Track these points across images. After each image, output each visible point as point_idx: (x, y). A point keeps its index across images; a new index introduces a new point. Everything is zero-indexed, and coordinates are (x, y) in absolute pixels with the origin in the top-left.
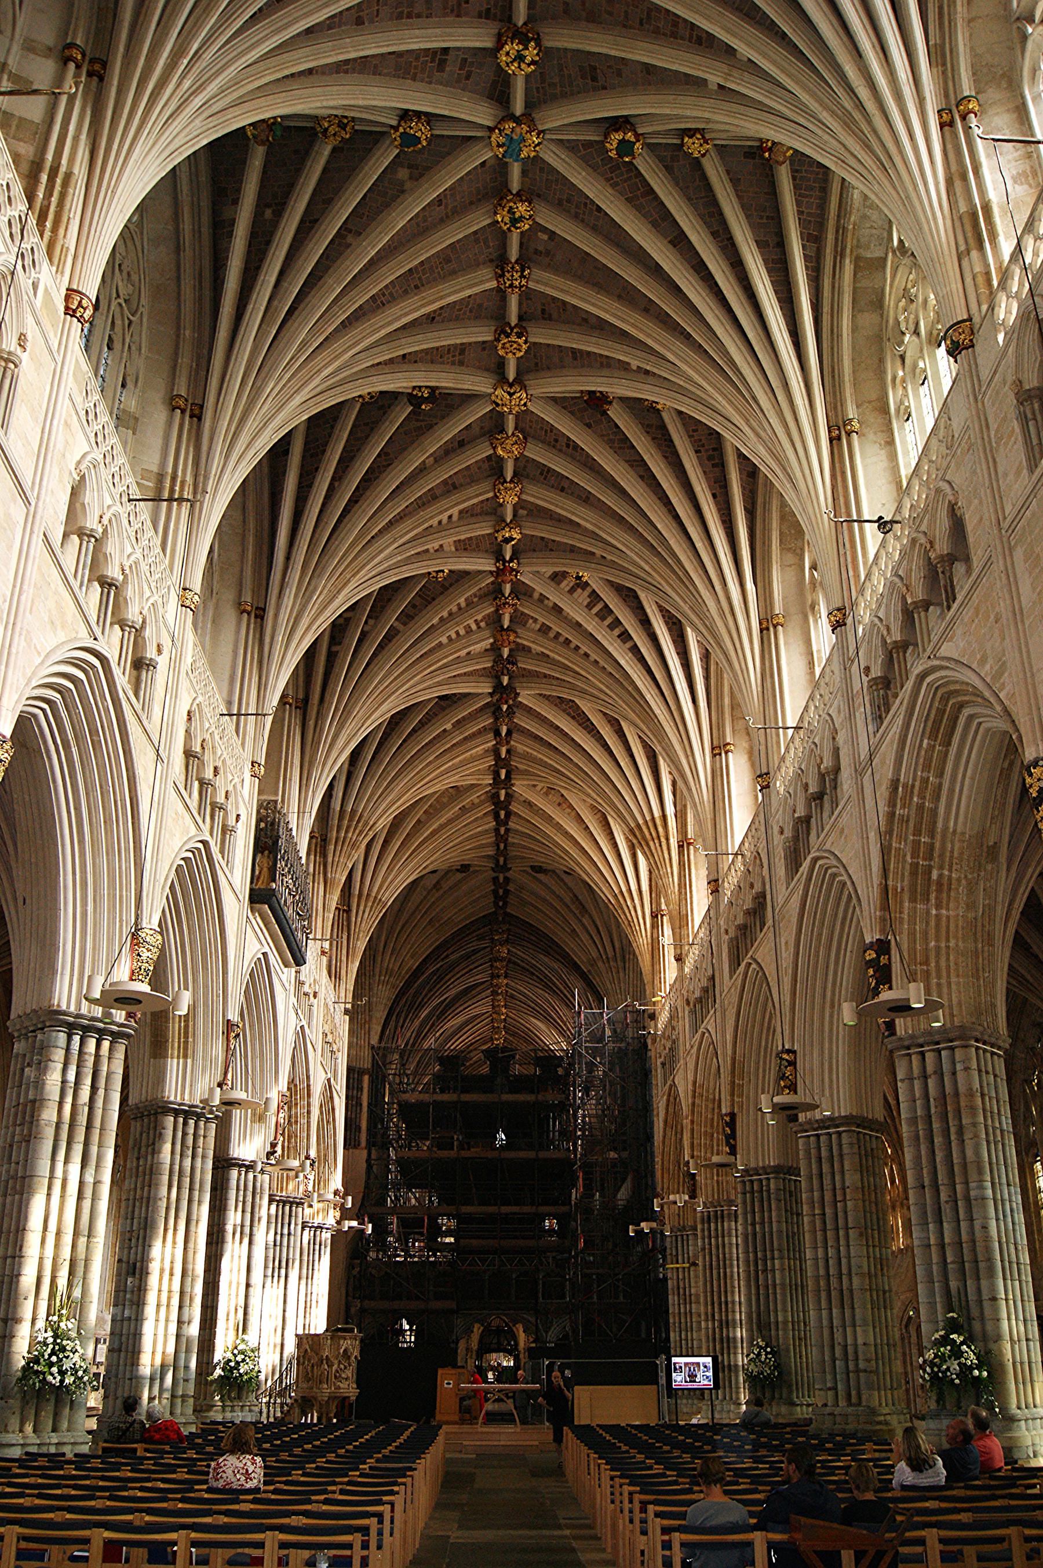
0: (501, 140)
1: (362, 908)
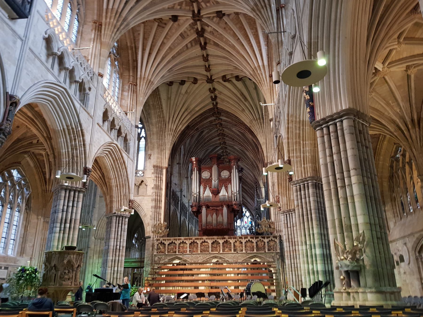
1: (142, 83)
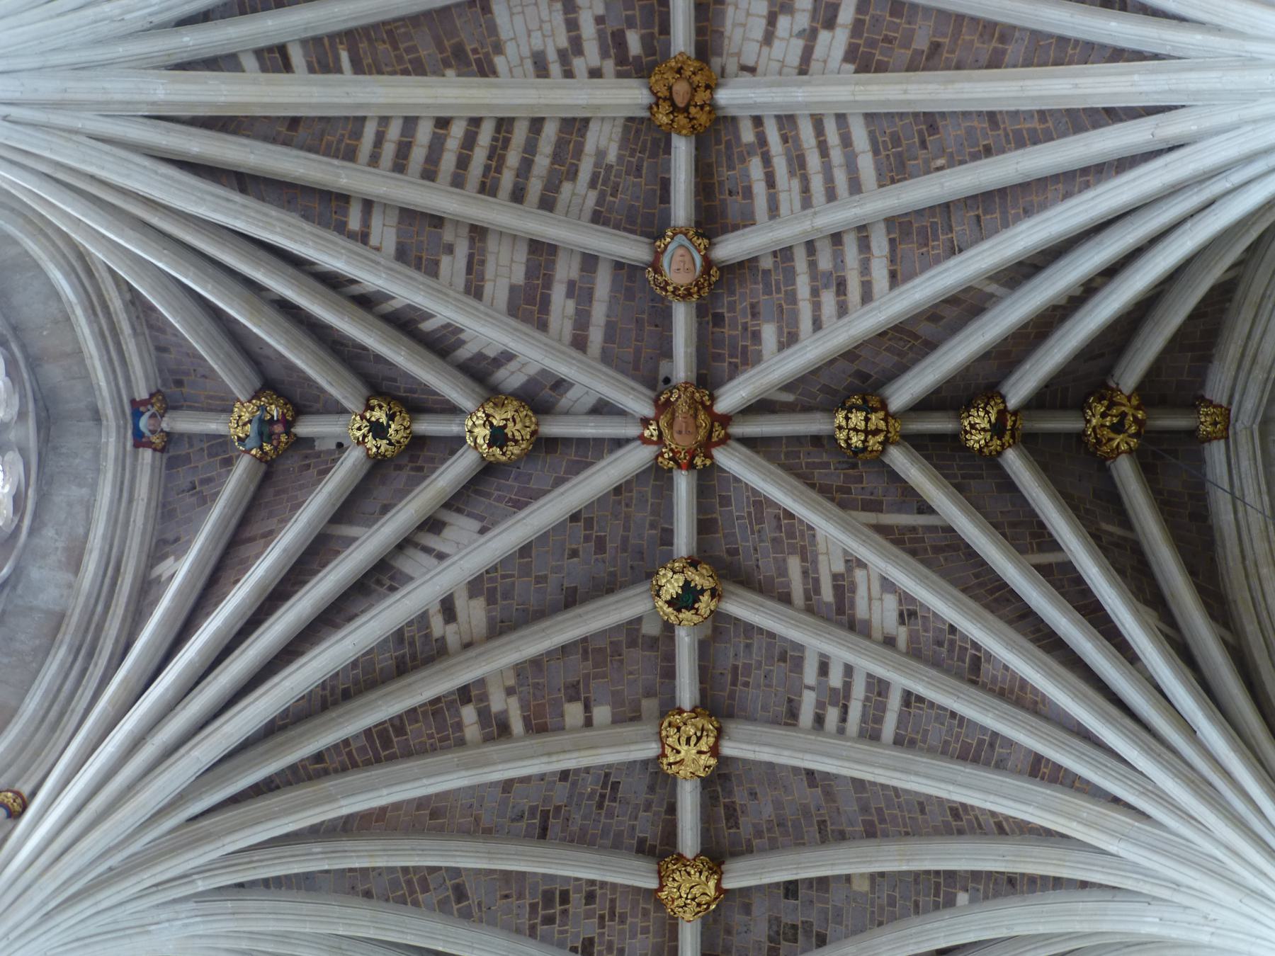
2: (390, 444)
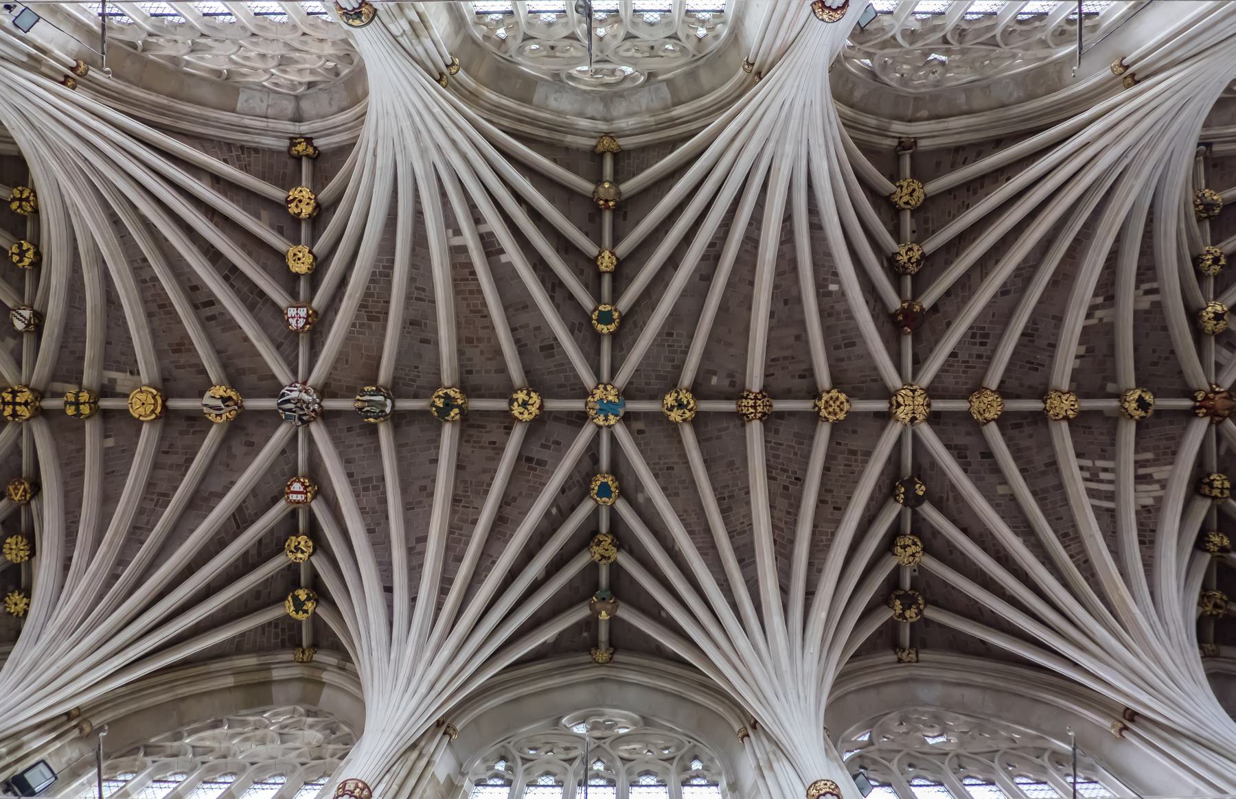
0: (602, 417)
2: (1210, 266)
